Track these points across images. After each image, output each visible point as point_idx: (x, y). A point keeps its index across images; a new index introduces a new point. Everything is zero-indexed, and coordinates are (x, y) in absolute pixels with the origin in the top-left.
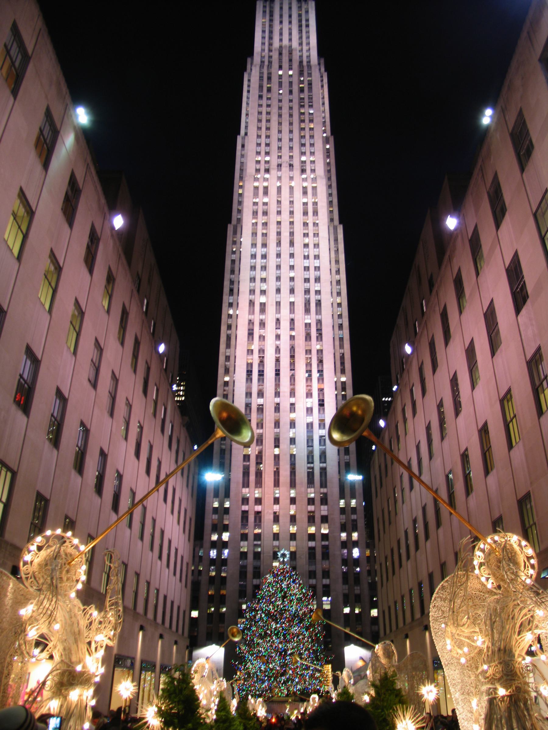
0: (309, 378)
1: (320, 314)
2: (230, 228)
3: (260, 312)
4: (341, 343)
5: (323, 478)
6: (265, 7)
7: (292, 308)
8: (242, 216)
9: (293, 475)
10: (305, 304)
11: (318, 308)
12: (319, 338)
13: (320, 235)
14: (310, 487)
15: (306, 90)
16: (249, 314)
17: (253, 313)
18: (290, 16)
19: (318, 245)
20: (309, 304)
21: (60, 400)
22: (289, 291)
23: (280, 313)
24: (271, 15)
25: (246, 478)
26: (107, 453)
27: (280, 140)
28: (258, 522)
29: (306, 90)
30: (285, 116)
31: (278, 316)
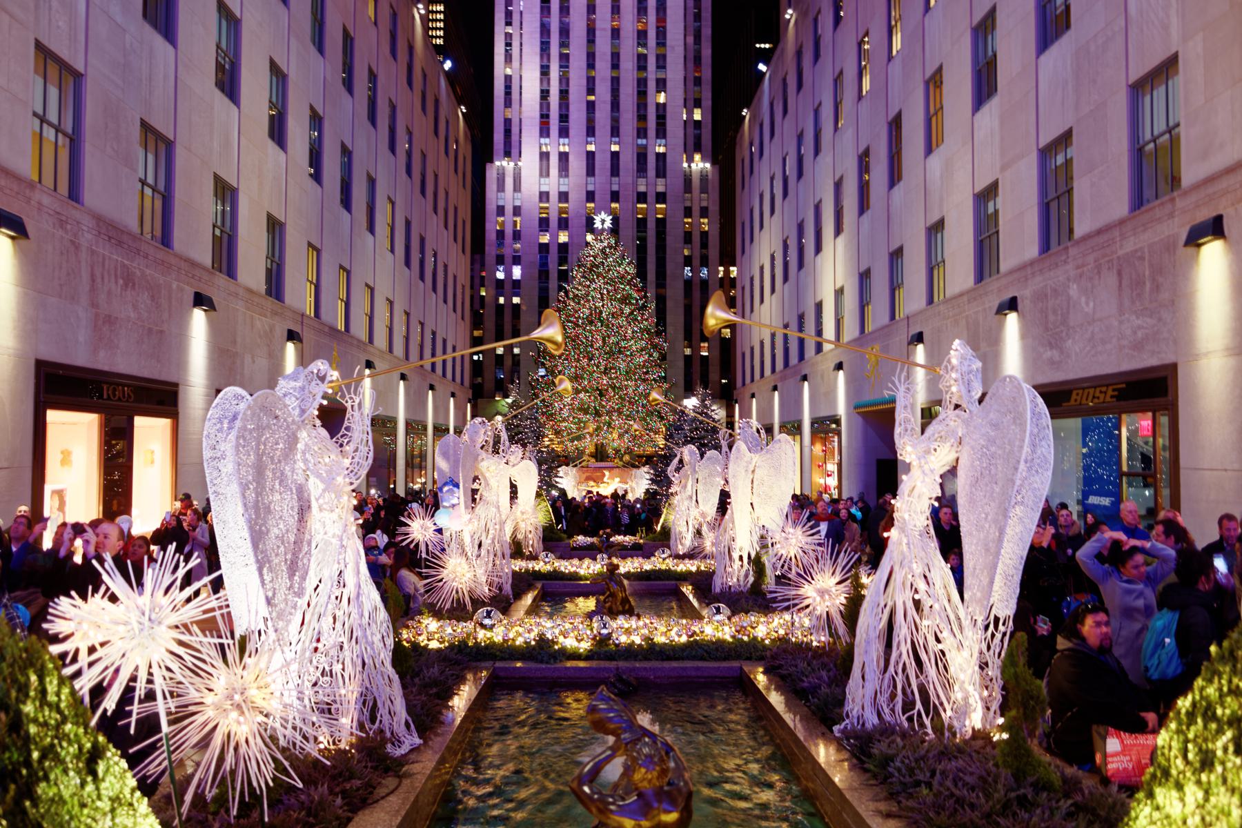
5: (661, 163)
21: (227, 20)
25: (545, 163)
26: (322, 114)
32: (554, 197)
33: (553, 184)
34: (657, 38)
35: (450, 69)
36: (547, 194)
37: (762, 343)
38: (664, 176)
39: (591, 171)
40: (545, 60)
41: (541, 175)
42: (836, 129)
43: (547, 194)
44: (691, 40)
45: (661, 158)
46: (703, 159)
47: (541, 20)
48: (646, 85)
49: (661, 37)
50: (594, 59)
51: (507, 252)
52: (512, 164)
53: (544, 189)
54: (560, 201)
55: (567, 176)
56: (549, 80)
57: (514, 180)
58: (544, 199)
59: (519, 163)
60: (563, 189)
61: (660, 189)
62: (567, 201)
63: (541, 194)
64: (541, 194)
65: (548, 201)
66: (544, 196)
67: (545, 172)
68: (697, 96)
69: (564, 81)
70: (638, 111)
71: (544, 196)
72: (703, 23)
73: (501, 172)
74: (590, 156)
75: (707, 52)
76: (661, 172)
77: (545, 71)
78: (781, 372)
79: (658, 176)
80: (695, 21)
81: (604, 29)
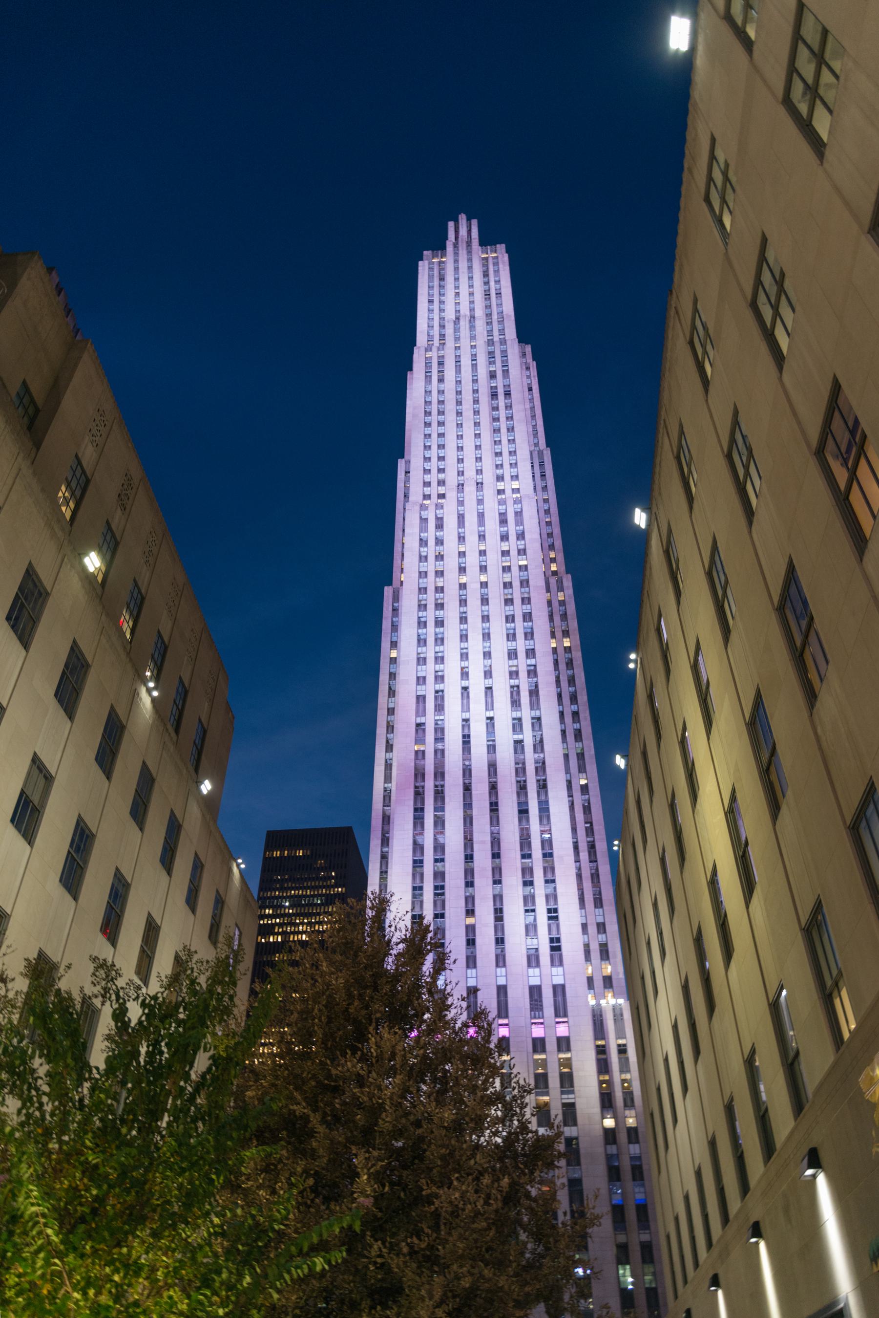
0: (523, 812)
1: (539, 709)
3: (436, 710)
5: (560, 998)
7: (489, 700)
9: (502, 995)
10: (512, 693)
11: (534, 698)
12: (538, 747)
13: (531, 583)
15: (499, 374)
16: (417, 715)
17: (424, 714)
18: (471, 278)
19: (529, 599)
20: (519, 692)
22: (483, 674)
23: (468, 711)
24: (442, 279)
29: (499, 374)
30: (468, 413)
31: (466, 715)
34: (543, 849)
40: (418, 880)
45: (559, 990)
46: (614, 996)
47: (414, 837)
49: (547, 847)
50: (473, 876)
56: (422, 902)
68: (600, 920)
69: (439, 903)
72: (596, 837)
76: (561, 1010)
77: (417, 890)
80: (587, 835)
81: (483, 842)
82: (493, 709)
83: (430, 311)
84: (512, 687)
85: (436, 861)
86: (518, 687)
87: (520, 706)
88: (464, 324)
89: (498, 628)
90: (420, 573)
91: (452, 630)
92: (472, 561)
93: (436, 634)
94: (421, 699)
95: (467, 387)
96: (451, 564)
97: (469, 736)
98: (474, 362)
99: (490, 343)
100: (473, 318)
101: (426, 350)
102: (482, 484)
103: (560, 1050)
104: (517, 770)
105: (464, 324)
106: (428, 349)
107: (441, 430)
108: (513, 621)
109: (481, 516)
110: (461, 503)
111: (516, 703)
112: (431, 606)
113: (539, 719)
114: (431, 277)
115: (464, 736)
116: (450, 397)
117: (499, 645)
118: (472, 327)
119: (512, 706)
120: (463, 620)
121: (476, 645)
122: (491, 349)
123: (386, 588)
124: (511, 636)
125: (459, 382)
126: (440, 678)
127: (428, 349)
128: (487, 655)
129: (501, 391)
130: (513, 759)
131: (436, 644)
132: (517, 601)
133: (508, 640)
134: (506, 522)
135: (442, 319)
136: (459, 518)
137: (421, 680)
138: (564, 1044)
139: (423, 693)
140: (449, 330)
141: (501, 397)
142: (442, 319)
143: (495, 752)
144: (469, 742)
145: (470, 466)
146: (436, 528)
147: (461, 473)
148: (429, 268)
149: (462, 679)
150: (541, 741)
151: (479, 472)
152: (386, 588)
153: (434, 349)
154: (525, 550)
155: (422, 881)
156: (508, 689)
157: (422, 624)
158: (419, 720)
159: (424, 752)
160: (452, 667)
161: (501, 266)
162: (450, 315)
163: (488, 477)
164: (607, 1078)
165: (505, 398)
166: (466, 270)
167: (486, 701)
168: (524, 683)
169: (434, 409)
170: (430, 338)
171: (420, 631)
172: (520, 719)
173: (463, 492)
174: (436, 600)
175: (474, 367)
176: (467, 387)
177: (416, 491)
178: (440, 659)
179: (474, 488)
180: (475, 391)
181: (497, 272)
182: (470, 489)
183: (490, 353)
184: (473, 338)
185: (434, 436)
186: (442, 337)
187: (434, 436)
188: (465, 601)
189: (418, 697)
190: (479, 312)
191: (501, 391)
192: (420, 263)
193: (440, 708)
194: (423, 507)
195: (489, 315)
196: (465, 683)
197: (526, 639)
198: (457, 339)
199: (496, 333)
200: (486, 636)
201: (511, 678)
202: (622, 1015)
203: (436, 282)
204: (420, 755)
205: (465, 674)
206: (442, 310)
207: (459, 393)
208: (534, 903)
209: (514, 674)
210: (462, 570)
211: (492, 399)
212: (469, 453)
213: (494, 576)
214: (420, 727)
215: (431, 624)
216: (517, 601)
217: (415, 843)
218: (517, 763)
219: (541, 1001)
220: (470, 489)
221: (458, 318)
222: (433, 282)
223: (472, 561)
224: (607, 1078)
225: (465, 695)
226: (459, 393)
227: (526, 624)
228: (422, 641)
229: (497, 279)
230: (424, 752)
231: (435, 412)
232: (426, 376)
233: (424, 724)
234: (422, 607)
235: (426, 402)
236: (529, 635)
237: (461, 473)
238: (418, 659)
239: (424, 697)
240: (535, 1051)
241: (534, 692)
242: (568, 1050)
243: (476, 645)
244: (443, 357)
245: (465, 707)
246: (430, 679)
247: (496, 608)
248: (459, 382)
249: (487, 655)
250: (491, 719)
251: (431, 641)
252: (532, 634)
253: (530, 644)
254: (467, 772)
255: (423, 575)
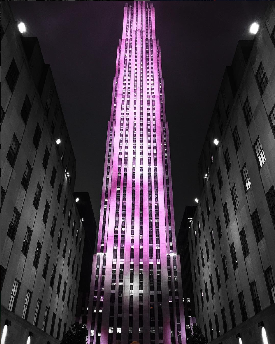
1: (157, 165)
2: (109, 122)
4: (167, 182)
6: (128, 10)
7: (141, 162)
8: (115, 117)
10: (148, 160)
11: (155, 162)
14: (150, 259)
17: (121, 165)
18: (142, 15)
24: (132, 14)
27: (136, 77)
28: (121, 278)
31: (134, 166)
32: (118, 267)
33: (118, 261)
34: (155, 209)
35: (78, 202)
36: (116, 265)
37: (210, 321)
38: (160, 258)
39: (132, 256)
41: (114, 258)
42: (236, 209)
43: (116, 265)
44: (167, 210)
47: (116, 203)
48: (152, 225)
51: (98, 290)
52: (103, 254)
53: (114, 263)
54: (120, 268)
55: (123, 258)
57: (104, 260)
58: (114, 267)
59: (106, 254)
60: (122, 263)
61: (158, 263)
62: (123, 268)
63: (113, 265)
64: (113, 265)
65: (116, 268)
66: (114, 266)
67: (115, 257)
70: (149, 234)
71: (114, 266)
73: (99, 257)
74: (132, 250)
75: (172, 215)
76: (158, 257)
78: (223, 335)
79: (157, 258)
81: (138, 206)
82: (142, 165)
83: (127, 26)
84: (149, 158)
85: (123, 210)
86: (151, 158)
87: (151, 164)
88: (139, 32)
89: (145, 139)
90: (121, 118)
91: (131, 138)
92: (138, 116)
93: (126, 139)
94: (120, 160)
95: (139, 56)
96: (131, 116)
97: (135, 172)
98: (142, 47)
99: (147, 40)
100: (141, 30)
101: (126, 41)
102: (142, 90)
103: (157, 269)
104: (149, 184)
105: (139, 32)
106: (126, 40)
107: (130, 70)
108: (150, 137)
109: (142, 101)
110: (135, 96)
111: (149, 163)
112: (124, 130)
113: (156, 168)
114: (128, 14)
115: (133, 172)
116: (133, 58)
117: (145, 144)
118: (141, 34)
119: (148, 164)
120: (134, 135)
121: (138, 144)
122: (147, 42)
123: (109, 121)
124: (149, 142)
125: (136, 53)
126: (126, 154)
127: (126, 40)
128: (141, 147)
129: (150, 58)
130: (148, 180)
131: (125, 143)
132: (152, 130)
133: (148, 143)
134: (150, 104)
135: (131, 29)
136: (134, 101)
137: (120, 154)
138: (159, 267)
139: (121, 158)
140: (134, 34)
141: (150, 60)
142: (131, 29)
143: (142, 178)
144: (134, 174)
145: (139, 83)
146: (127, 104)
147: (135, 86)
148: (128, 10)
149: (133, 154)
150: (157, 175)
151: (141, 86)
152: (109, 121)
153: (128, 40)
154: (155, 114)
155: (118, 216)
156: (147, 158)
157: (121, 136)
158: (119, 166)
159: (120, 176)
160: (130, 150)
161: (152, 12)
162: (134, 28)
163: (144, 88)
164: (170, 277)
165: (151, 61)
166: (140, 12)
167: (140, 162)
168: (153, 157)
169: (128, 62)
170: (127, 36)
171: (121, 138)
172: (151, 168)
173: (136, 92)
174: (126, 128)
175: (142, 48)
176: (139, 56)
177: (120, 91)
178: (126, 147)
179: (140, 91)
180: (142, 57)
181: (150, 14)
182: (138, 91)
183: (147, 44)
184: (142, 38)
185: (127, 72)
186: (131, 36)
187: (127, 72)
188: (135, 129)
189: (119, 159)
190: (144, 29)
191: (150, 58)
192: (125, 8)
193: (126, 163)
194: (123, 96)
195: (147, 30)
196: (134, 156)
197: (154, 143)
198: (136, 38)
199: (149, 36)
200: (141, 141)
201: (148, 155)
202: (176, 259)
203: (130, 16)
204: (119, 177)
205: (134, 153)
206: (131, 26)
207: (136, 57)
208: (152, 225)
209: (149, 154)
210: (135, 119)
211: (147, 60)
212: (139, 79)
213: (145, 122)
214: (119, 169)
215: (124, 136)
216: (152, 130)
217: (117, 204)
218: (149, 182)
219: (153, 254)
220: (138, 91)
221: (137, 30)
222: (129, 15)
223: (138, 116)
224: (170, 277)
225: (134, 159)
226: (136, 57)
227: (154, 138)
228: (121, 141)
229: (150, 16)
230: (120, 176)
231: (128, 63)
232: (125, 50)
233: (121, 168)
234: (121, 130)
235: (125, 59)
236: (155, 142)
237: (135, 86)
238: (120, 147)
239: (121, 159)
240: (150, 268)
241: (155, 160)
242: (160, 269)
243: (138, 144)
244: (131, 43)
245: (134, 164)
246: (123, 154)
247: (145, 132)
248: (136, 53)
249: (141, 147)
250: (142, 168)
251: (124, 141)
252: (156, 141)
253: (155, 145)
254: (134, 183)
255: (122, 119)
